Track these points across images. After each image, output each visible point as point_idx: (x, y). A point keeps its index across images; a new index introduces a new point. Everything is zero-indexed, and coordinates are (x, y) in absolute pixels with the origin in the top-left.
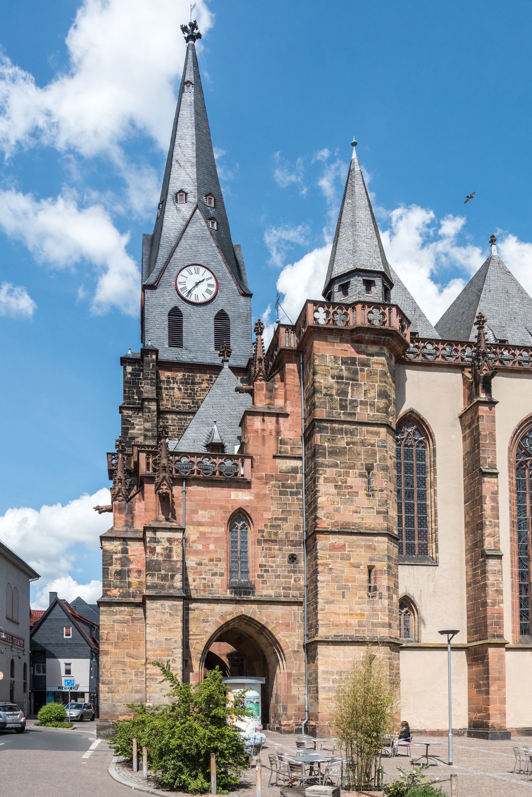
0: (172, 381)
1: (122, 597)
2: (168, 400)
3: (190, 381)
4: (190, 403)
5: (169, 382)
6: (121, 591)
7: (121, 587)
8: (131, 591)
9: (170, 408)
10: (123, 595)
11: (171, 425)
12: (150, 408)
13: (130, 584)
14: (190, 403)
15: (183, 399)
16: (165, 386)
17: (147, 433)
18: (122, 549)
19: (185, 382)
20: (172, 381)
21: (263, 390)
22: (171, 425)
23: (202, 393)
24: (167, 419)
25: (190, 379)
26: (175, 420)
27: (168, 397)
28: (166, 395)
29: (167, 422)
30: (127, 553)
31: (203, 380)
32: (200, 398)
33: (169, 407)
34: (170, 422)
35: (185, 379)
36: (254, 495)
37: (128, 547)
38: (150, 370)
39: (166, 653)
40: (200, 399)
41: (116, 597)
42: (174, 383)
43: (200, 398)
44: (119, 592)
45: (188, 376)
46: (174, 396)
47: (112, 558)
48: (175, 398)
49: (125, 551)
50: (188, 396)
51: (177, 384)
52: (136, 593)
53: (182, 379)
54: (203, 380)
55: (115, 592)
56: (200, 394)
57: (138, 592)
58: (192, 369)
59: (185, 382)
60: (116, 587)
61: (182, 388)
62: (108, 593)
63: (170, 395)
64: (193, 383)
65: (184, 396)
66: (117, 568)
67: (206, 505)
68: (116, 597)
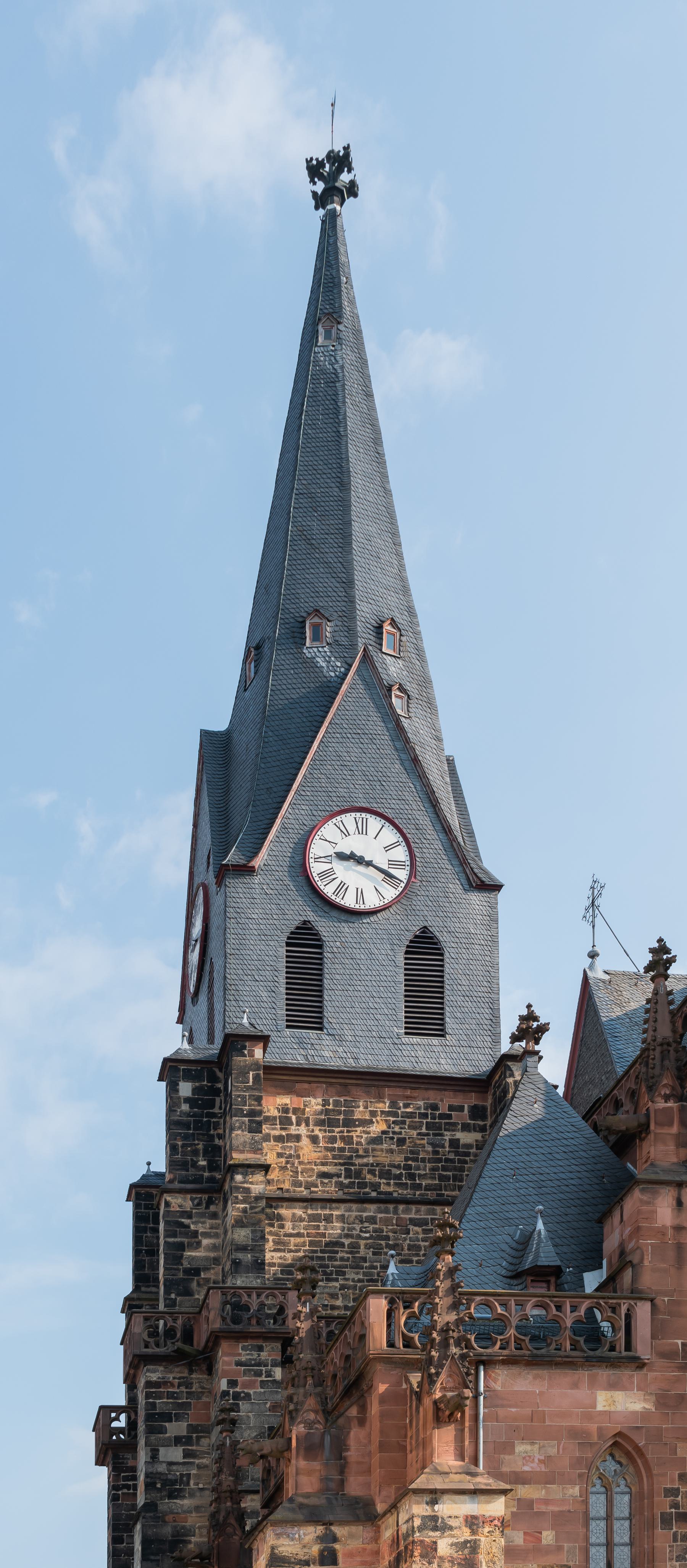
0: (294, 1118)
2: (283, 1169)
3: (342, 1117)
4: (339, 1176)
5: (285, 1122)
9: (288, 1191)
11: (291, 1235)
12: (248, 1190)
14: (339, 1176)
15: (323, 1164)
16: (277, 1133)
17: (240, 1255)
19: (327, 1121)
20: (294, 1118)
21: (671, 1124)
22: (291, 1235)
23: (370, 1147)
24: (280, 1218)
25: (340, 1113)
26: (301, 1220)
27: (283, 1160)
28: (280, 1155)
29: (282, 1227)
31: (373, 1114)
32: (365, 1160)
33: (286, 1186)
34: (288, 1225)
35: (327, 1112)
36: (653, 1398)
38: (249, 1088)
40: (367, 1165)
42: (298, 1124)
43: (365, 1160)
45: (336, 1103)
46: (298, 1157)
48: (300, 1163)
50: (334, 1157)
51: (307, 1125)
53: (321, 1113)
54: (373, 1114)
56: (366, 1151)
58: (346, 1085)
59: (327, 1121)
61: (321, 1136)
63: (290, 1156)
64: (349, 1123)
65: (325, 1157)
67: (534, 1427)
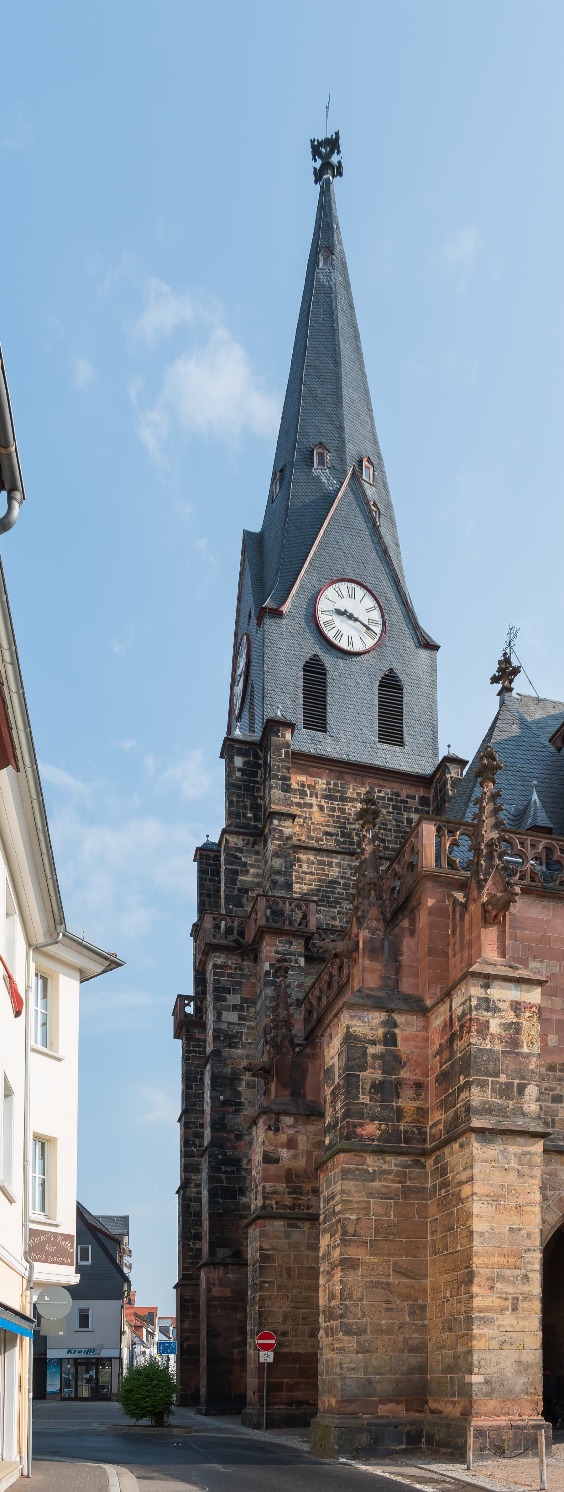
1: (385, 1141)
6: (383, 1127)
7: (382, 1120)
8: (402, 1128)
10: (386, 1137)
13: (400, 1111)
18: (385, 1035)
30: (395, 1044)
37: (397, 1031)
39: (512, 1260)
41: (374, 1140)
44: (379, 1129)
47: (365, 1054)
49: (390, 1039)
52: (413, 1132)
55: (371, 1129)
57: (416, 1131)
60: (372, 1119)
62: (359, 1130)
66: (375, 1076)
68: (374, 1140)
